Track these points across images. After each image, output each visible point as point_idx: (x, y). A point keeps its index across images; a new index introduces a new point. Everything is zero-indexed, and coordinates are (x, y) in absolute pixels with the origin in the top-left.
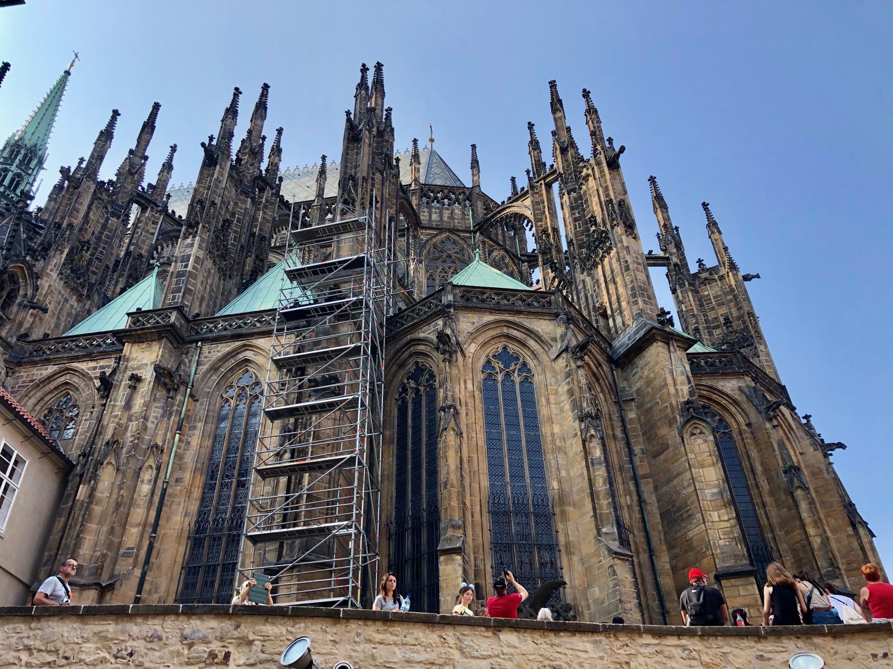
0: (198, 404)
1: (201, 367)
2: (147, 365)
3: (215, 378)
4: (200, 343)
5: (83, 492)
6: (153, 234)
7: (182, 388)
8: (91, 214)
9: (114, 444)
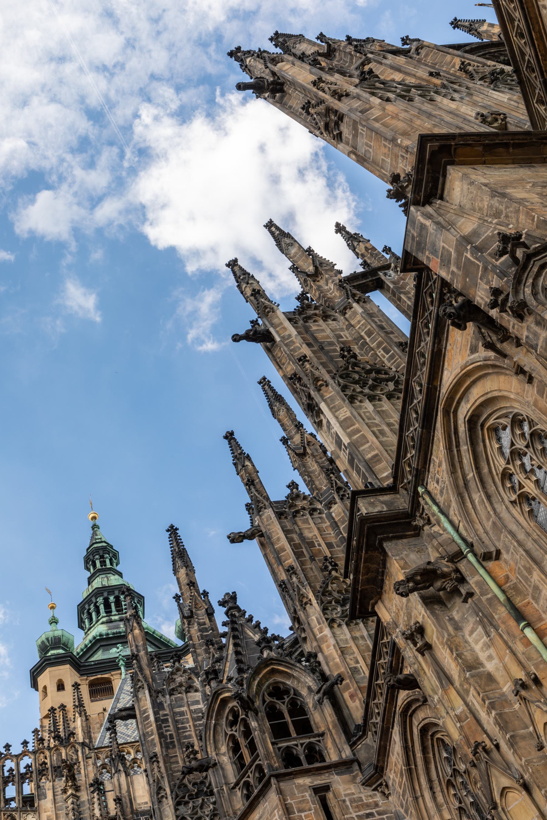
1: (451, 513)
3: (478, 496)
7: (462, 566)
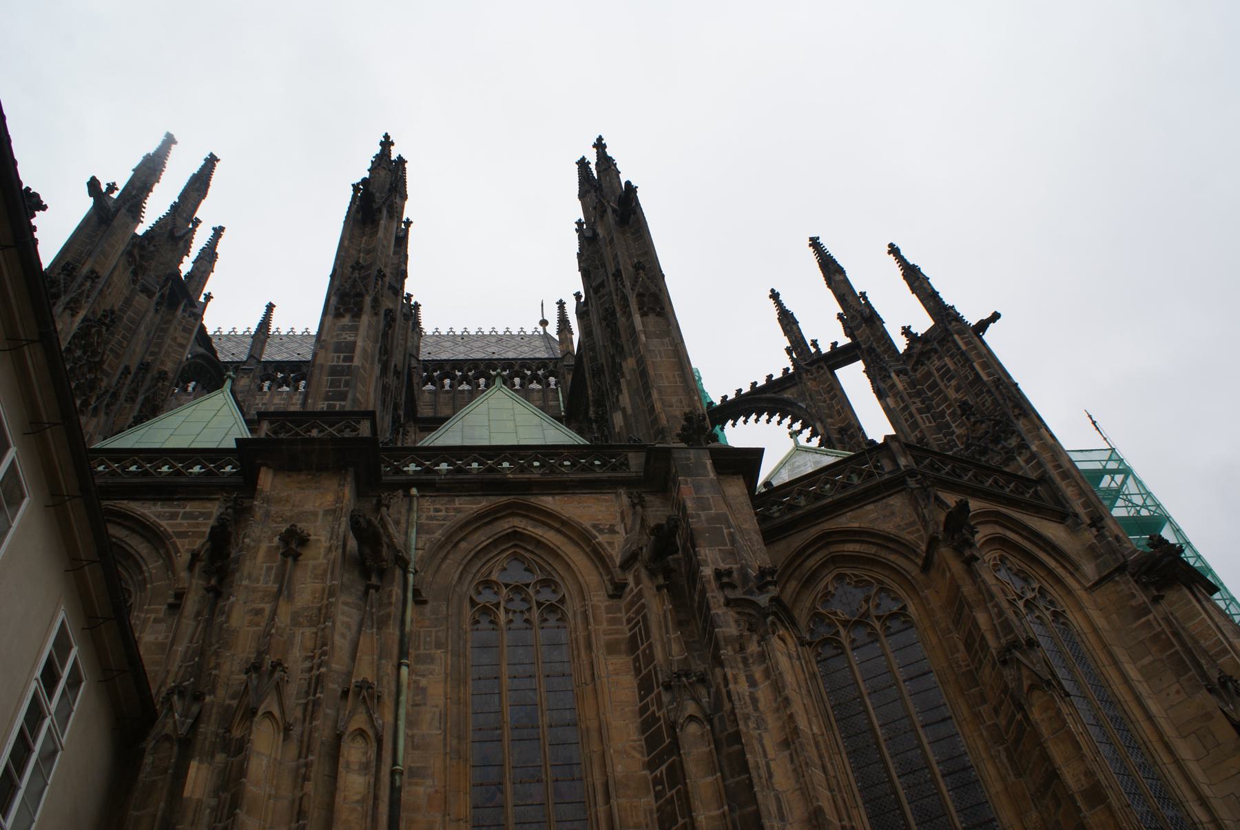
0: (428, 608)
2: (315, 514)
4: (414, 491)
5: (199, 779)
6: (183, 346)
8: (116, 273)
9: (265, 668)
